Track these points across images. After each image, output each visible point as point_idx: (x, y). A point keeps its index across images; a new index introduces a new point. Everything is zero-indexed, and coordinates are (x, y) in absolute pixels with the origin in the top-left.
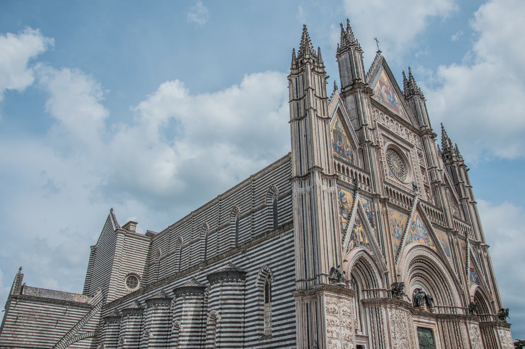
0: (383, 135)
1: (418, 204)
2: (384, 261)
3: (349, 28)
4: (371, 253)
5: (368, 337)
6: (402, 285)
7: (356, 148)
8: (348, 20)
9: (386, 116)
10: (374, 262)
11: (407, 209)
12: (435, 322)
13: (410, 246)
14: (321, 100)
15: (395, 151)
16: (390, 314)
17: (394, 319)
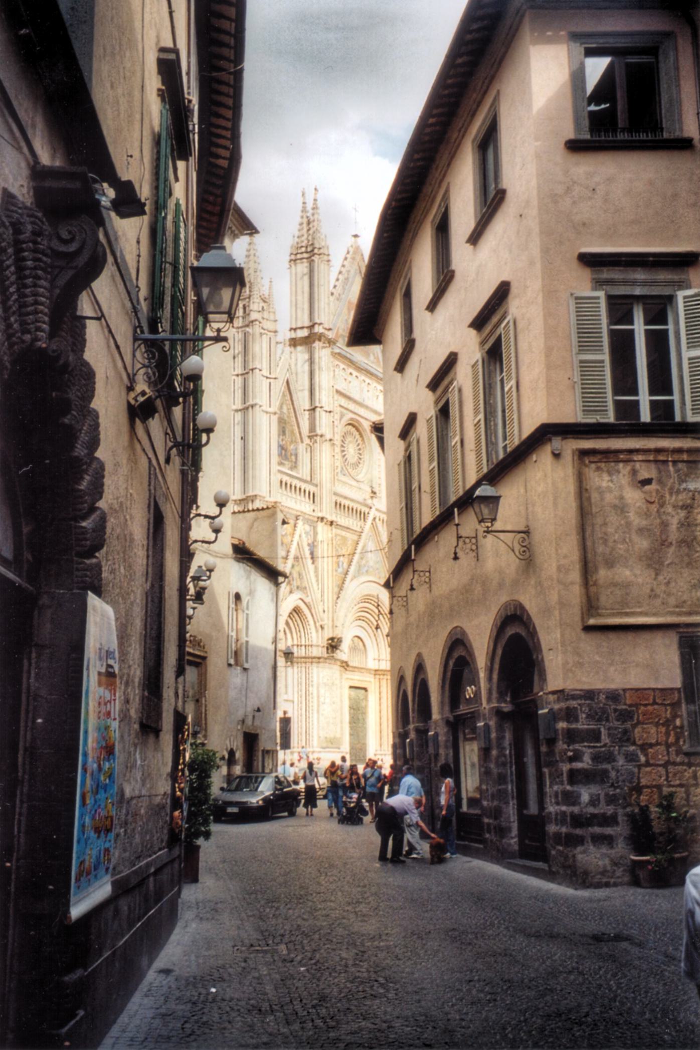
0: (341, 406)
1: (374, 519)
2: (321, 610)
3: (315, 208)
4: (307, 600)
5: (293, 702)
6: (340, 640)
7: (302, 442)
8: (316, 189)
9: (351, 370)
10: (310, 609)
11: (359, 529)
12: (372, 680)
13: (356, 582)
14: (268, 381)
15: (354, 426)
16: (321, 675)
17: (325, 681)
